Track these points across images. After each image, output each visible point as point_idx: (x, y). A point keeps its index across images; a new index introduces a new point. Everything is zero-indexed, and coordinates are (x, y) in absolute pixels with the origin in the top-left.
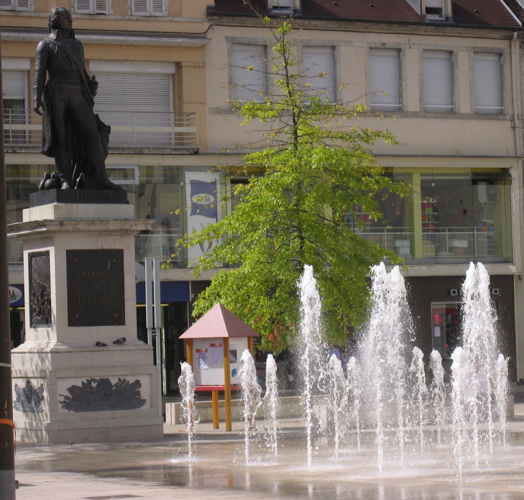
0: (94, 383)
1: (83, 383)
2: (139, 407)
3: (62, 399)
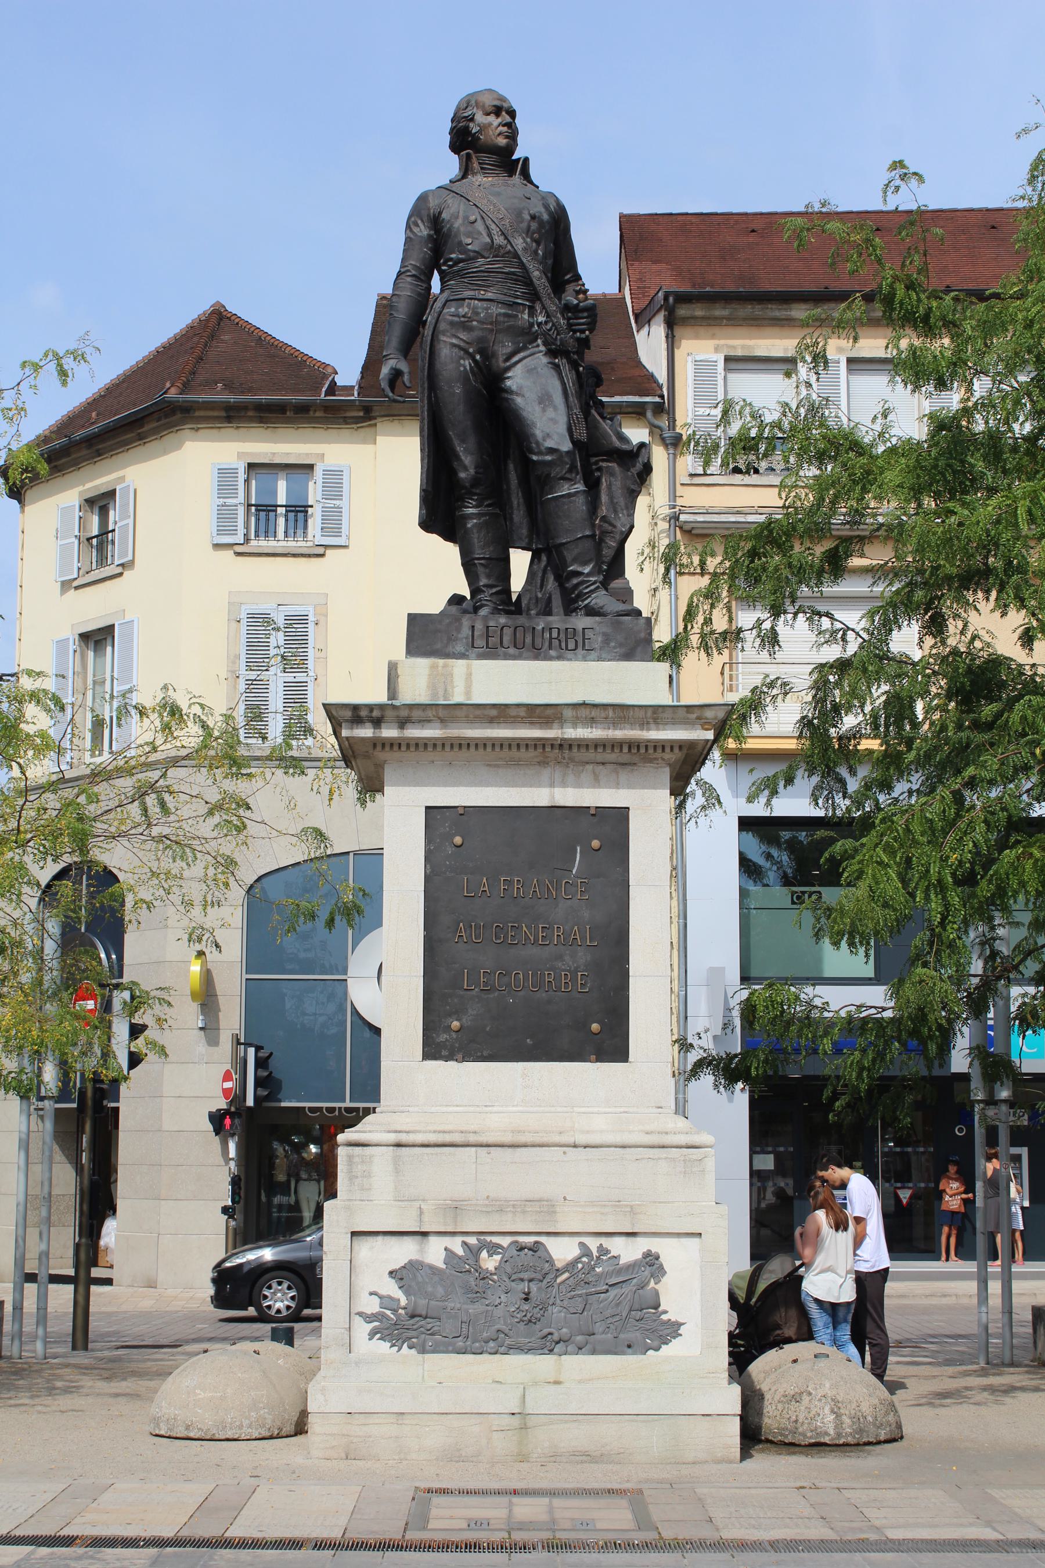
0: (490, 1255)
2: (657, 1349)
3: (373, 1306)
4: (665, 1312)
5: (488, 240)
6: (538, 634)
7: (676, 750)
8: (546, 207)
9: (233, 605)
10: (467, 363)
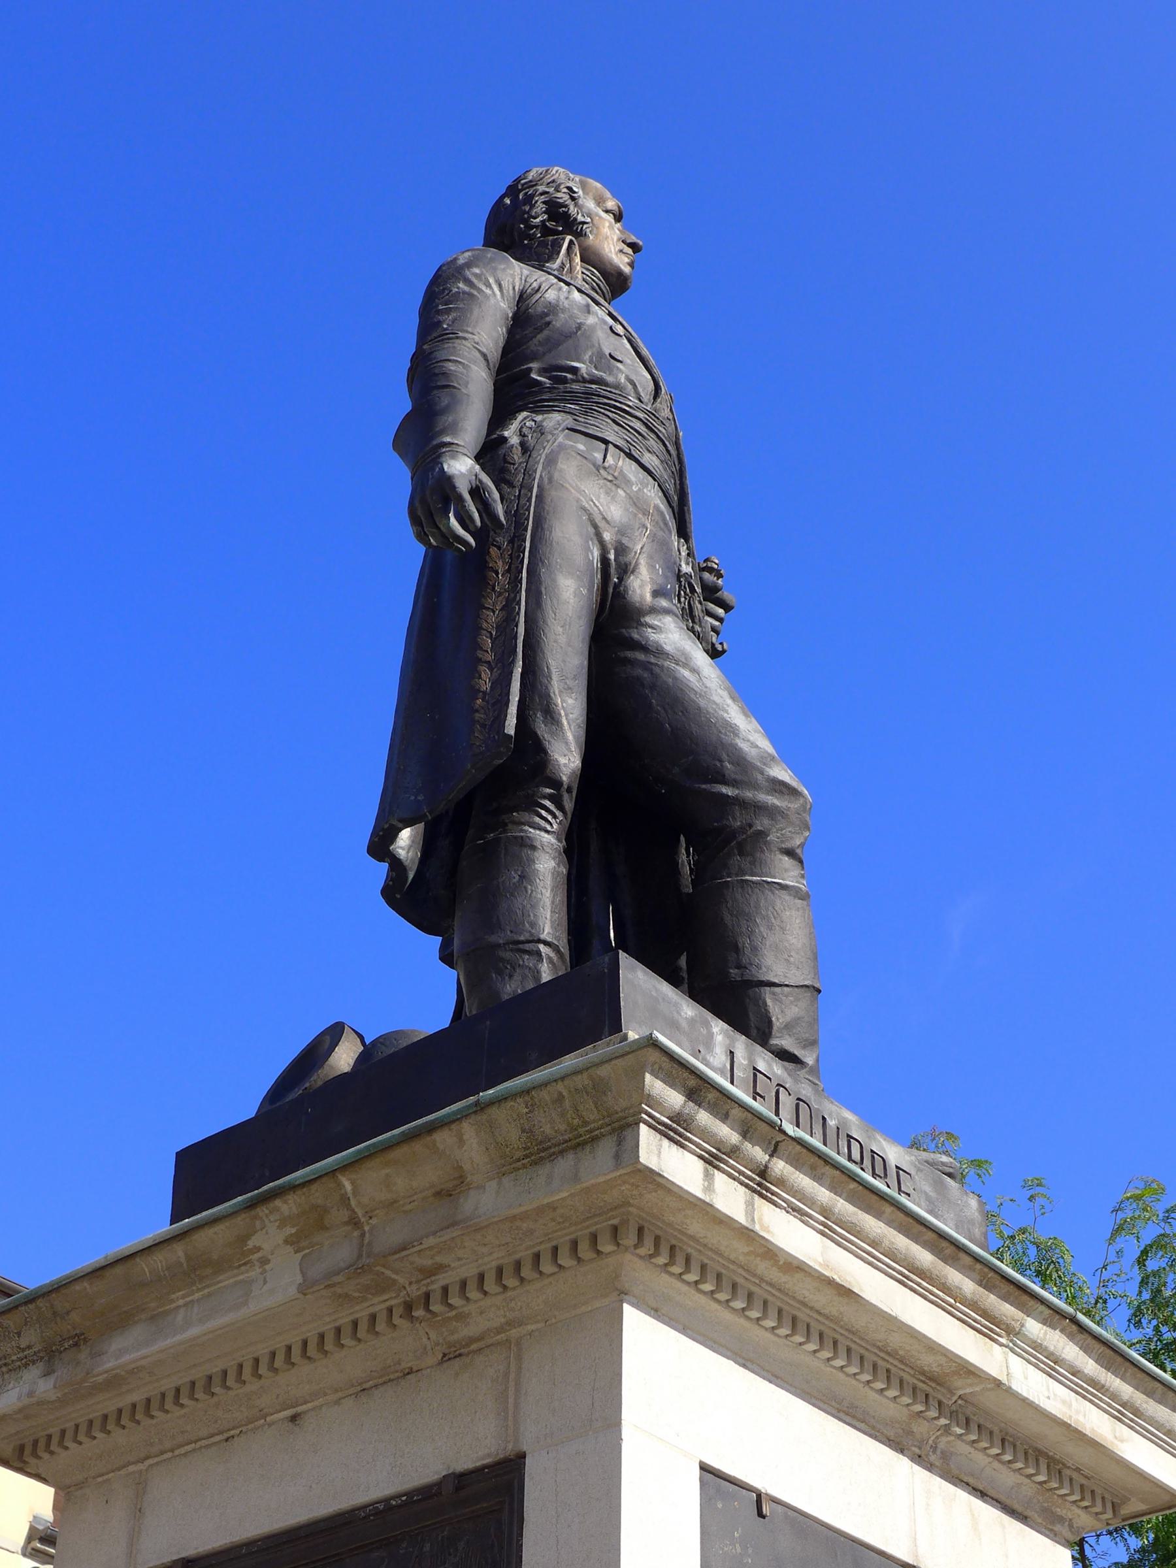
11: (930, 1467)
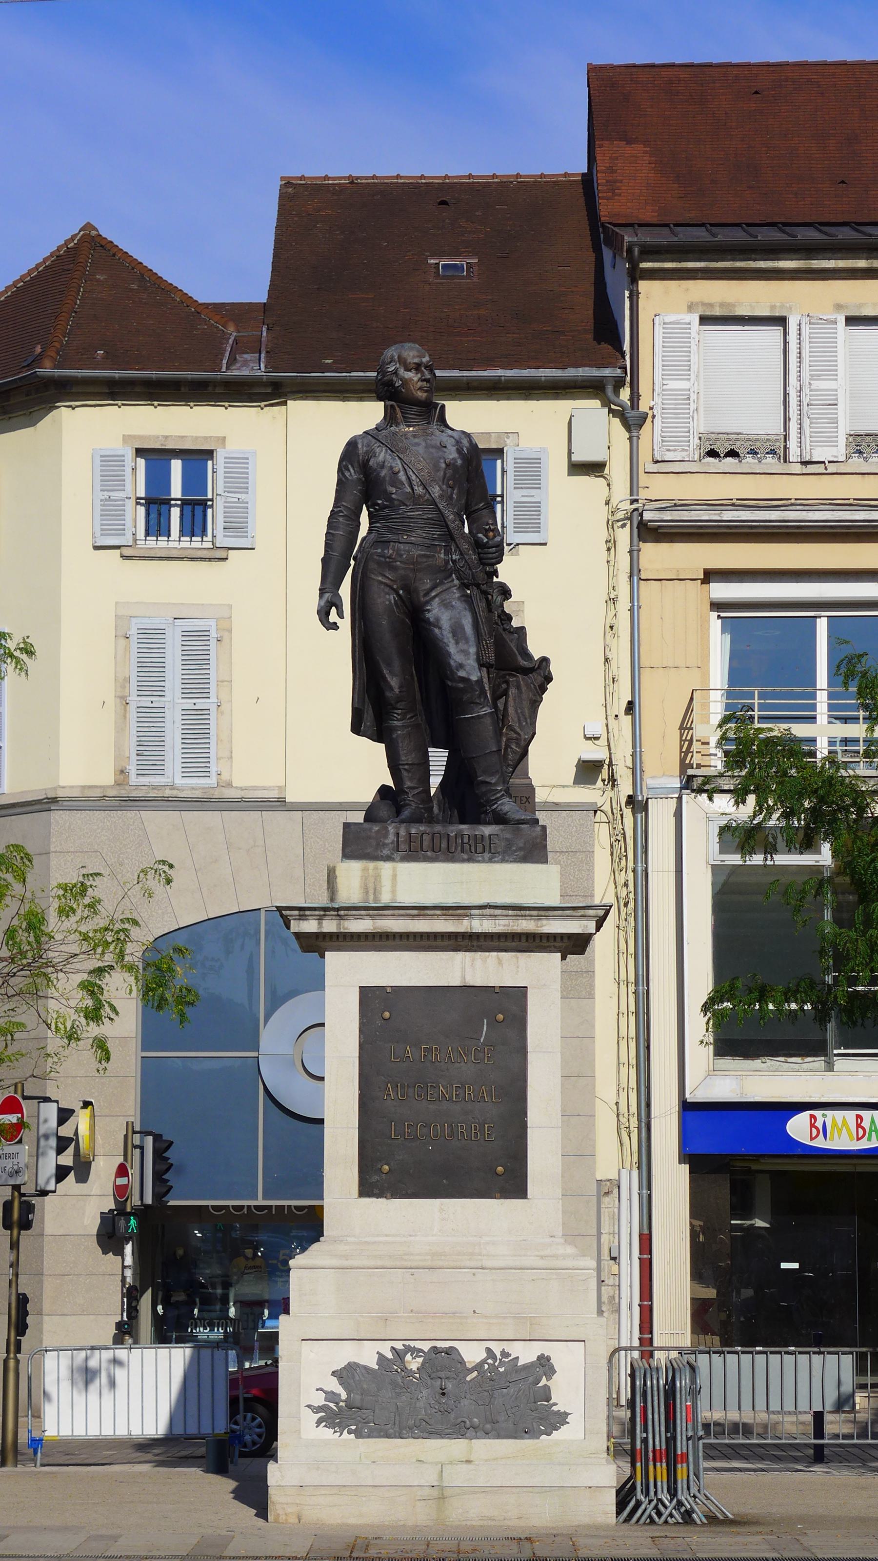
1: (381, 1357)
3: (319, 1400)
4: (556, 1404)
5: (409, 490)
6: (452, 840)
7: (565, 940)
8: (459, 451)
9: (121, 619)
10: (392, 597)
11: (475, 951)
